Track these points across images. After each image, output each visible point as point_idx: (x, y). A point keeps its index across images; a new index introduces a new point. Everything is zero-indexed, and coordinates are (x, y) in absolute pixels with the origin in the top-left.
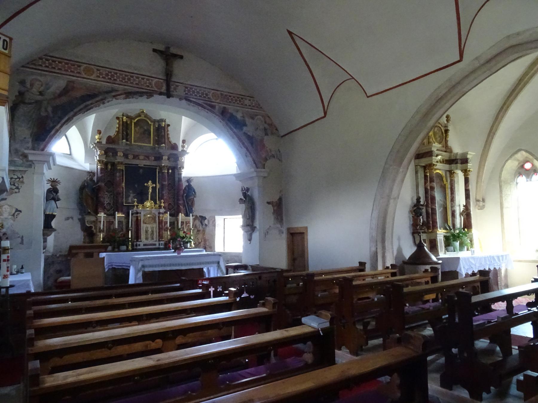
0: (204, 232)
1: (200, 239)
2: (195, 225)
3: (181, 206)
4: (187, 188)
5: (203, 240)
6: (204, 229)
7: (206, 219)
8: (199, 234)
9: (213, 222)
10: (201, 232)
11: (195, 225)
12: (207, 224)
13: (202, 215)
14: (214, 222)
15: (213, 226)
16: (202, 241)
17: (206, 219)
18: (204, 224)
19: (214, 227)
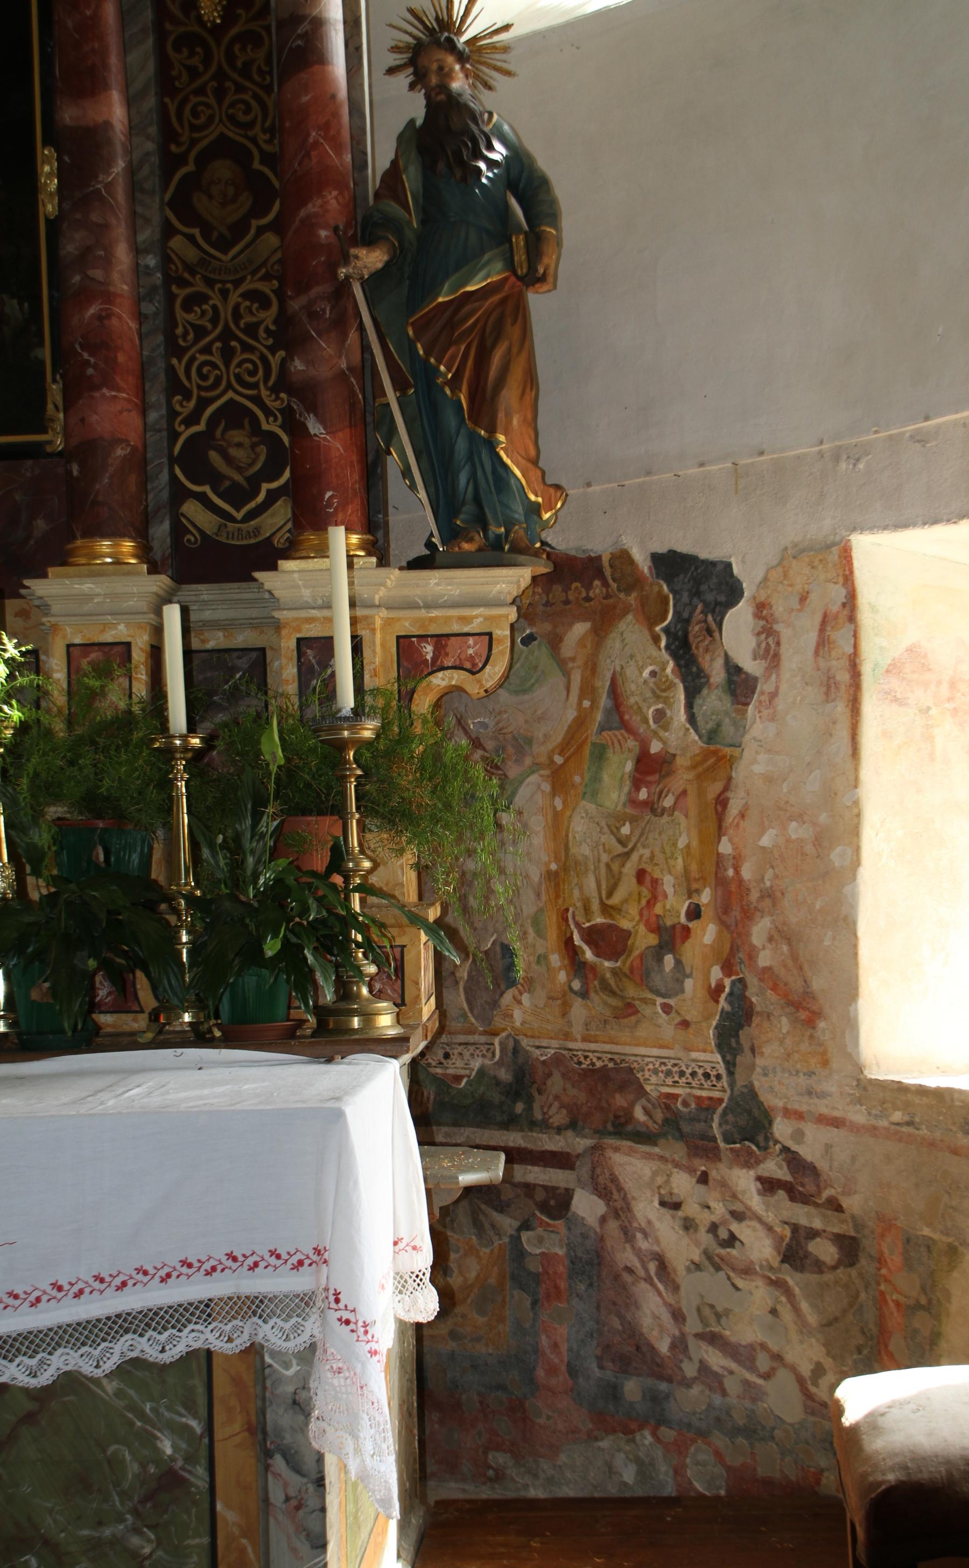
0: (714, 789)
1: (668, 884)
2: (614, 691)
3: (314, 427)
4: (411, 180)
5: (705, 897)
6: (712, 736)
7: (733, 592)
8: (651, 806)
9: (823, 643)
10: (682, 778)
11: (614, 691)
12: (750, 666)
13: (684, 547)
14: (841, 637)
15: (829, 686)
16: (695, 913)
17: (733, 592)
18: (717, 673)
19: (840, 708)
